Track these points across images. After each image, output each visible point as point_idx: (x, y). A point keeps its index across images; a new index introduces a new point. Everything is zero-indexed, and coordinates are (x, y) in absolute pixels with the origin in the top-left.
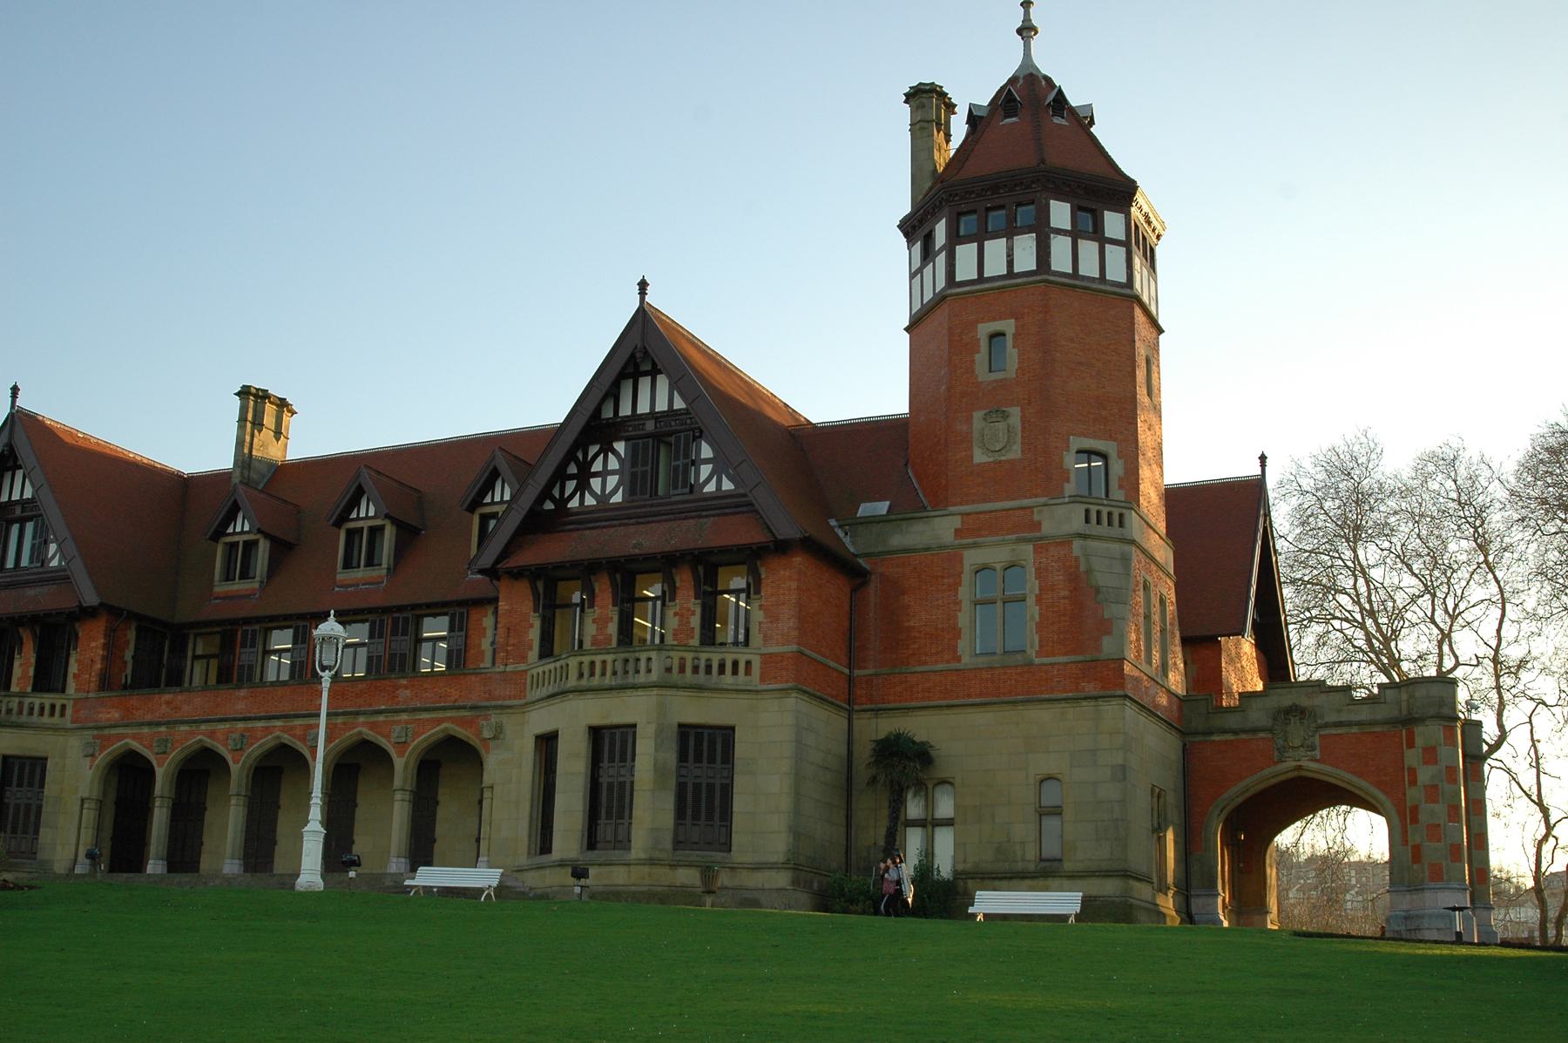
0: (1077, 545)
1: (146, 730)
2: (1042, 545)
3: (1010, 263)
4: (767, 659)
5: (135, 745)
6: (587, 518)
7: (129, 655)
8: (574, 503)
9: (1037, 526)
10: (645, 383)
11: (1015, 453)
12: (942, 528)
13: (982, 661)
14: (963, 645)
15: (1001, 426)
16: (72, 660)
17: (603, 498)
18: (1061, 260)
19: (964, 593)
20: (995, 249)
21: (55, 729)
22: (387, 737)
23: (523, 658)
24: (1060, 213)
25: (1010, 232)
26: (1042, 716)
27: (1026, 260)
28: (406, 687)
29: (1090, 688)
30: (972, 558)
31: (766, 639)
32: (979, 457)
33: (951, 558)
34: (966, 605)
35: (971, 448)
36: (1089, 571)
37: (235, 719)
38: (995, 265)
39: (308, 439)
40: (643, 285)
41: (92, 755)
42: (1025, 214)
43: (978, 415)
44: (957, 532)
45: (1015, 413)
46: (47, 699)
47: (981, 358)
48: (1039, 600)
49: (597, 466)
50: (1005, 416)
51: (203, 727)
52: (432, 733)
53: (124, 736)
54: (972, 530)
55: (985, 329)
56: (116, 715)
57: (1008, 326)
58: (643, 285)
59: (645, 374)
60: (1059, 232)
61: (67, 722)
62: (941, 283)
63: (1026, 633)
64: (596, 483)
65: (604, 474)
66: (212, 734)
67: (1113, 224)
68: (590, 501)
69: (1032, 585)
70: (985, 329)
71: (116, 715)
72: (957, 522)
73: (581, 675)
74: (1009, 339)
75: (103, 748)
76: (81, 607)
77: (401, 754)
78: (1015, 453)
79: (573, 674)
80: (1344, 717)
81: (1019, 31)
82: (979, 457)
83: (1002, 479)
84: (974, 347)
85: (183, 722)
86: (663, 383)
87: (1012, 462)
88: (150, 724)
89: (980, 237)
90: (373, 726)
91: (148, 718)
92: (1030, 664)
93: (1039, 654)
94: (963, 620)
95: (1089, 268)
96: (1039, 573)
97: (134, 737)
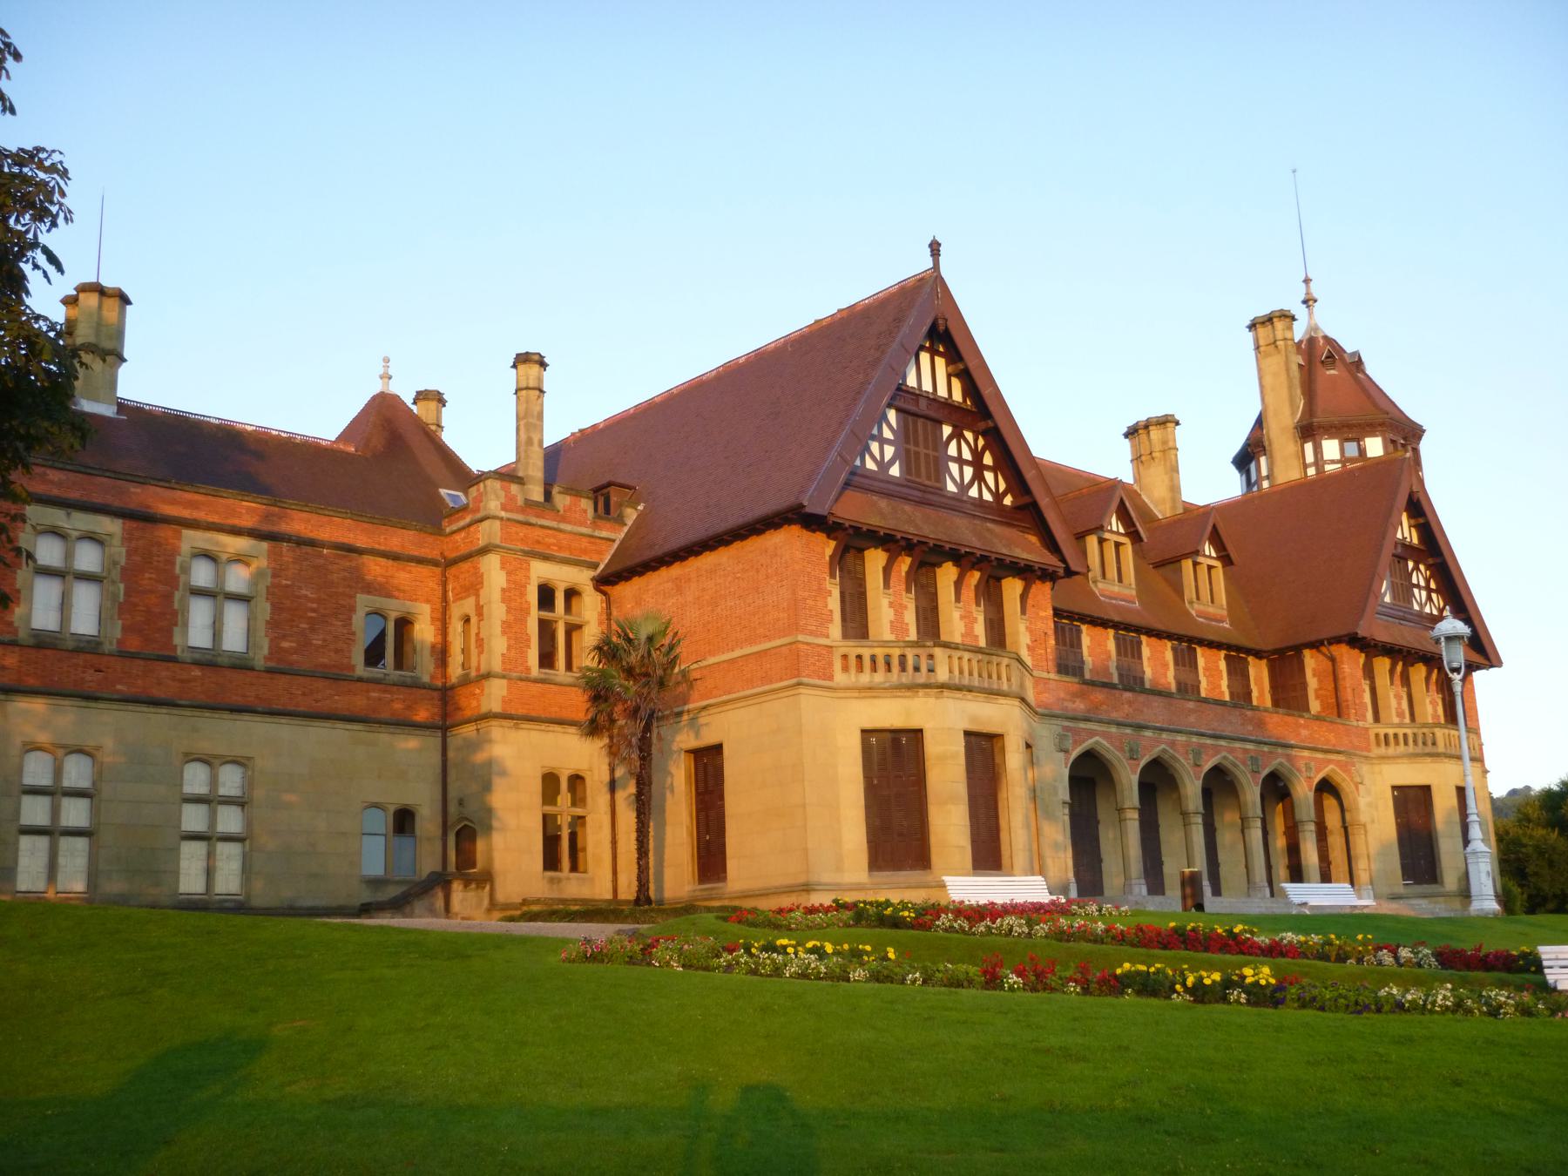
1: (1113, 729)
23: (1364, 718)
28: (1306, 727)
37: (1192, 733)
41: (1066, 751)
51: (1164, 736)
53: (1092, 733)
75: (1076, 743)
81: (1305, 302)
85: (1147, 728)
88: (1119, 724)
97: (1104, 735)
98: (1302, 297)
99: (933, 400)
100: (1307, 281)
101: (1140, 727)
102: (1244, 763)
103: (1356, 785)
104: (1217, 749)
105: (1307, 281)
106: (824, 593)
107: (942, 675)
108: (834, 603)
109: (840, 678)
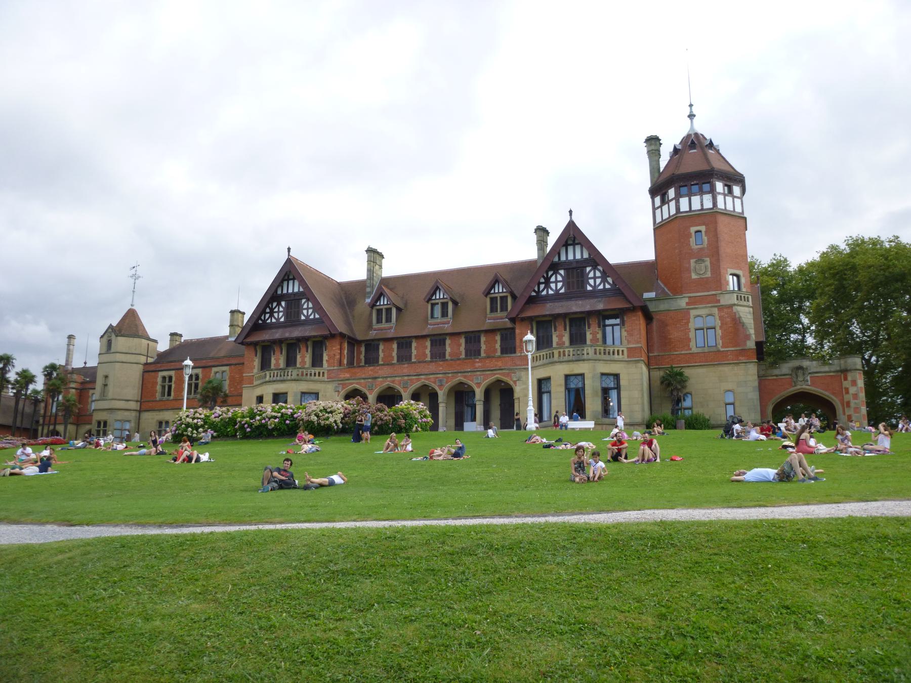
0: (735, 308)
2: (721, 308)
3: (702, 205)
4: (629, 349)
5: (358, 387)
6: (548, 298)
7: (346, 352)
8: (544, 293)
9: (719, 301)
10: (570, 249)
11: (709, 274)
12: (682, 303)
13: (699, 350)
14: (692, 344)
15: (703, 265)
16: (325, 355)
17: (557, 291)
18: (720, 205)
19: (692, 326)
20: (696, 200)
21: (321, 382)
22: (472, 381)
24: (719, 186)
25: (701, 193)
26: (726, 369)
27: (708, 204)
29: (743, 359)
30: (693, 313)
31: (629, 342)
32: (694, 276)
33: (685, 313)
34: (693, 331)
35: (690, 273)
36: (740, 317)
38: (696, 205)
39: (390, 269)
40: (571, 212)
42: (706, 187)
43: (692, 261)
44: (687, 304)
45: (708, 262)
46: (317, 370)
47: (692, 240)
48: (721, 328)
49: (553, 279)
50: (703, 261)
52: (492, 379)
53: (352, 384)
54: (693, 302)
55: (693, 229)
56: (347, 375)
57: (703, 228)
58: (571, 212)
59: (570, 245)
60: (719, 193)
61: (325, 378)
62: (673, 211)
63: (715, 339)
64: (553, 286)
65: (556, 282)
66: (393, 382)
67: (737, 190)
68: (551, 292)
69: (718, 323)
70: (693, 229)
71: (347, 375)
72: (687, 300)
73: (560, 356)
74: (703, 233)
75: (343, 388)
76: (331, 334)
77: (478, 387)
78: (709, 274)
79: (556, 355)
80: (815, 370)
81: (689, 116)
82: (694, 276)
83: (703, 284)
84: (689, 235)
86: (578, 248)
87: (707, 278)
89: (690, 195)
90: (465, 377)
91: (363, 376)
92: (719, 351)
93: (722, 347)
94: (692, 335)
95: (730, 207)
96: (721, 318)
98: (688, 114)
99: (294, 294)
100: (691, 106)
101: (376, 378)
102: (435, 383)
103: (515, 382)
104: (418, 380)
105: (691, 106)
106: (253, 361)
107: (267, 379)
108: (257, 362)
109: (255, 383)
